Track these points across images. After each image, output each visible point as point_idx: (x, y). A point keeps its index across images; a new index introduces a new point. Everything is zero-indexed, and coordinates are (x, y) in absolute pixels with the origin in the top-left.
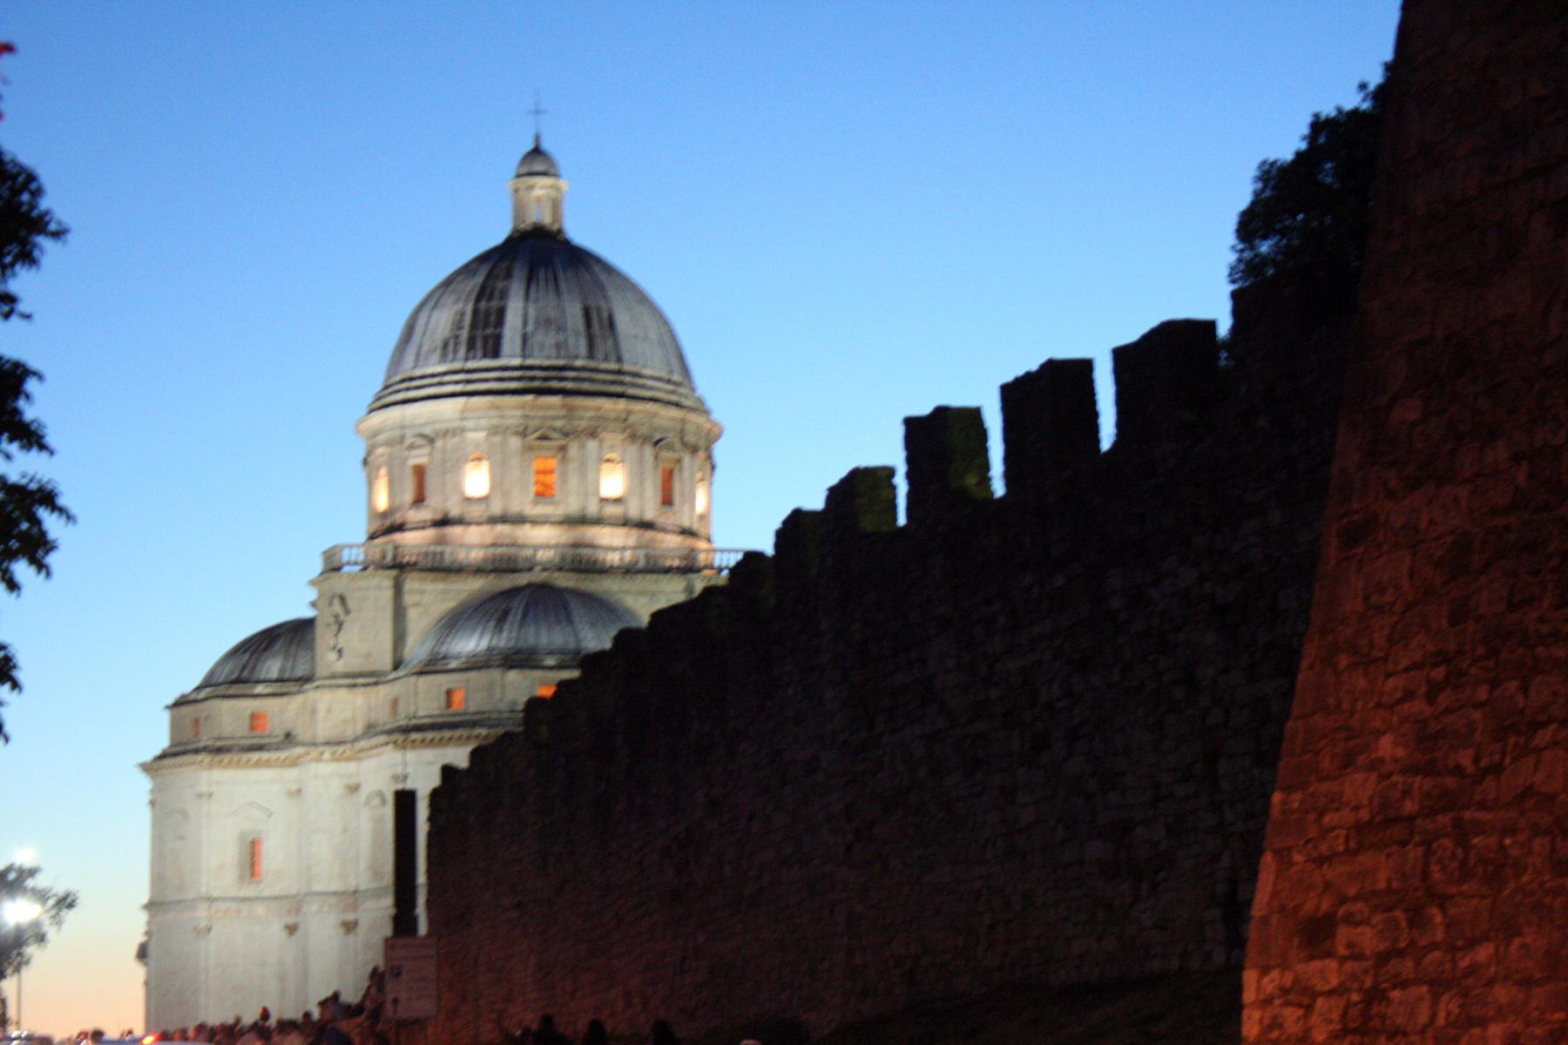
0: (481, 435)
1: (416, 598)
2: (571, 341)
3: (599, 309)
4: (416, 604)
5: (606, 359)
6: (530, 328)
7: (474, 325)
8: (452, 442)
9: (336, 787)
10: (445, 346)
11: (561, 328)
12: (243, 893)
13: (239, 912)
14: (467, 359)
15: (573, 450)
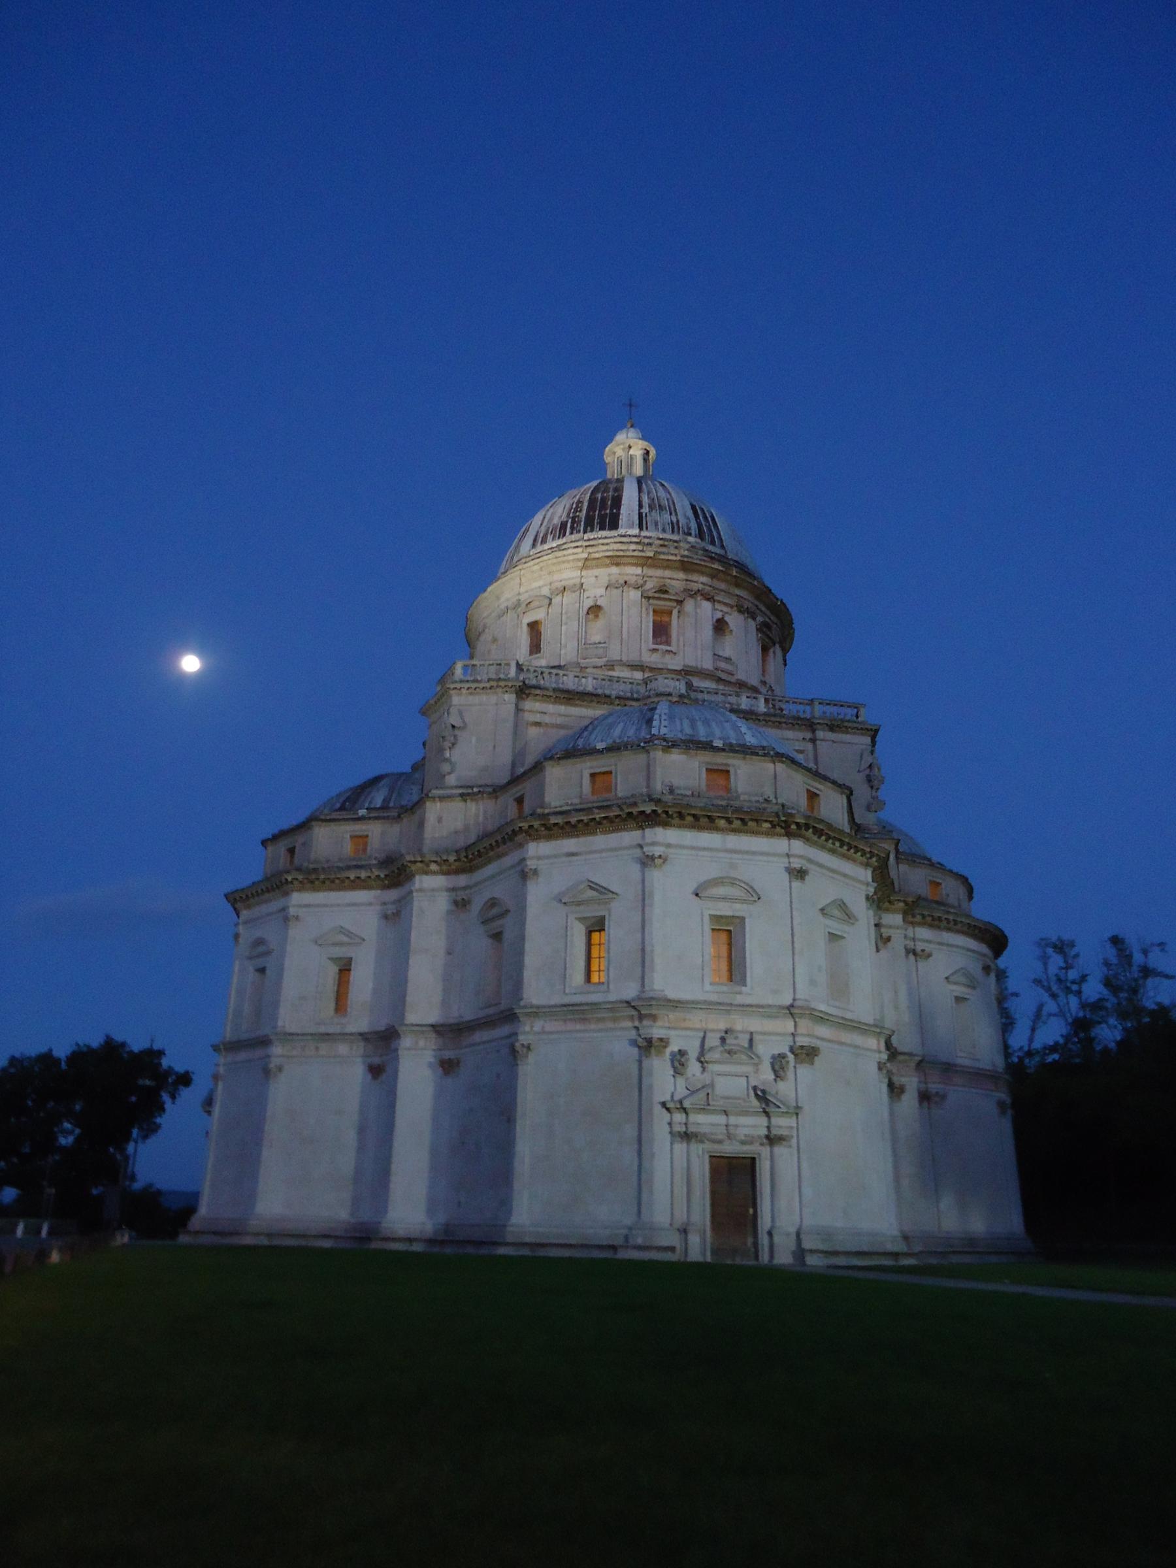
0: (602, 591)
1: (538, 718)
2: (682, 521)
3: (702, 510)
4: (537, 724)
5: (713, 543)
6: (645, 510)
7: (592, 506)
8: (569, 598)
9: (442, 903)
10: (563, 526)
11: (673, 511)
12: (322, 1029)
13: (317, 1049)
14: (585, 532)
15: (689, 605)
